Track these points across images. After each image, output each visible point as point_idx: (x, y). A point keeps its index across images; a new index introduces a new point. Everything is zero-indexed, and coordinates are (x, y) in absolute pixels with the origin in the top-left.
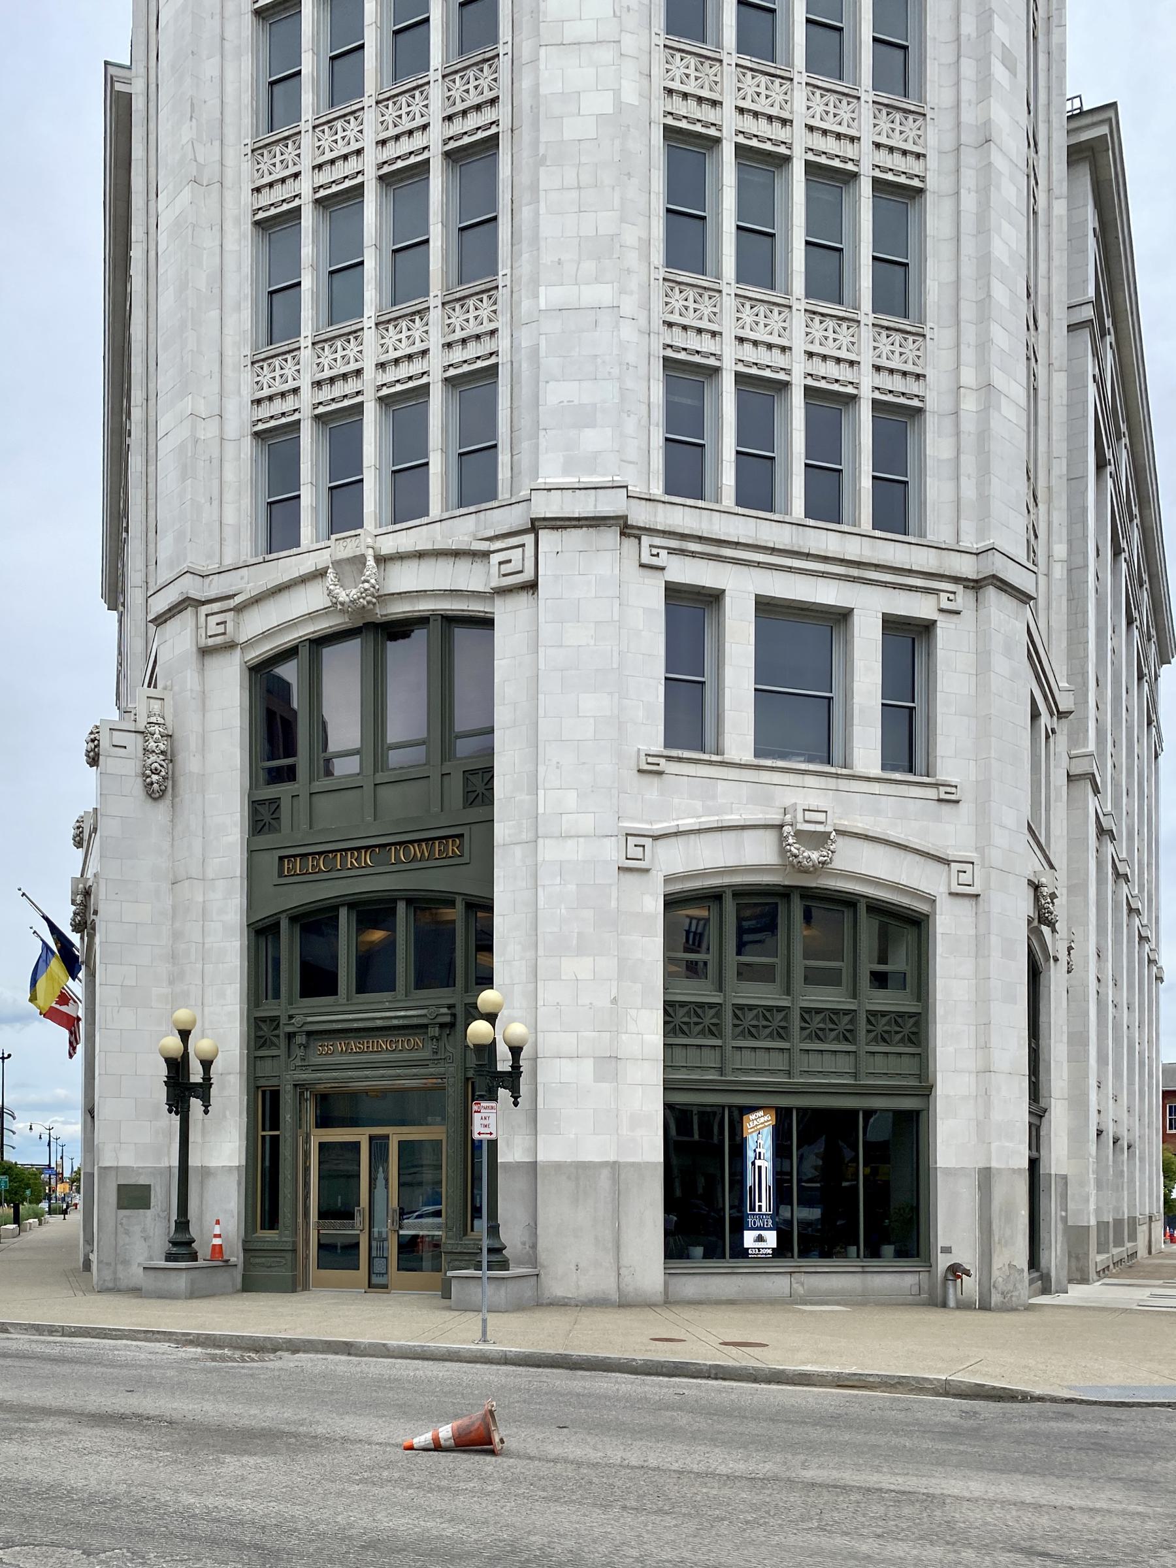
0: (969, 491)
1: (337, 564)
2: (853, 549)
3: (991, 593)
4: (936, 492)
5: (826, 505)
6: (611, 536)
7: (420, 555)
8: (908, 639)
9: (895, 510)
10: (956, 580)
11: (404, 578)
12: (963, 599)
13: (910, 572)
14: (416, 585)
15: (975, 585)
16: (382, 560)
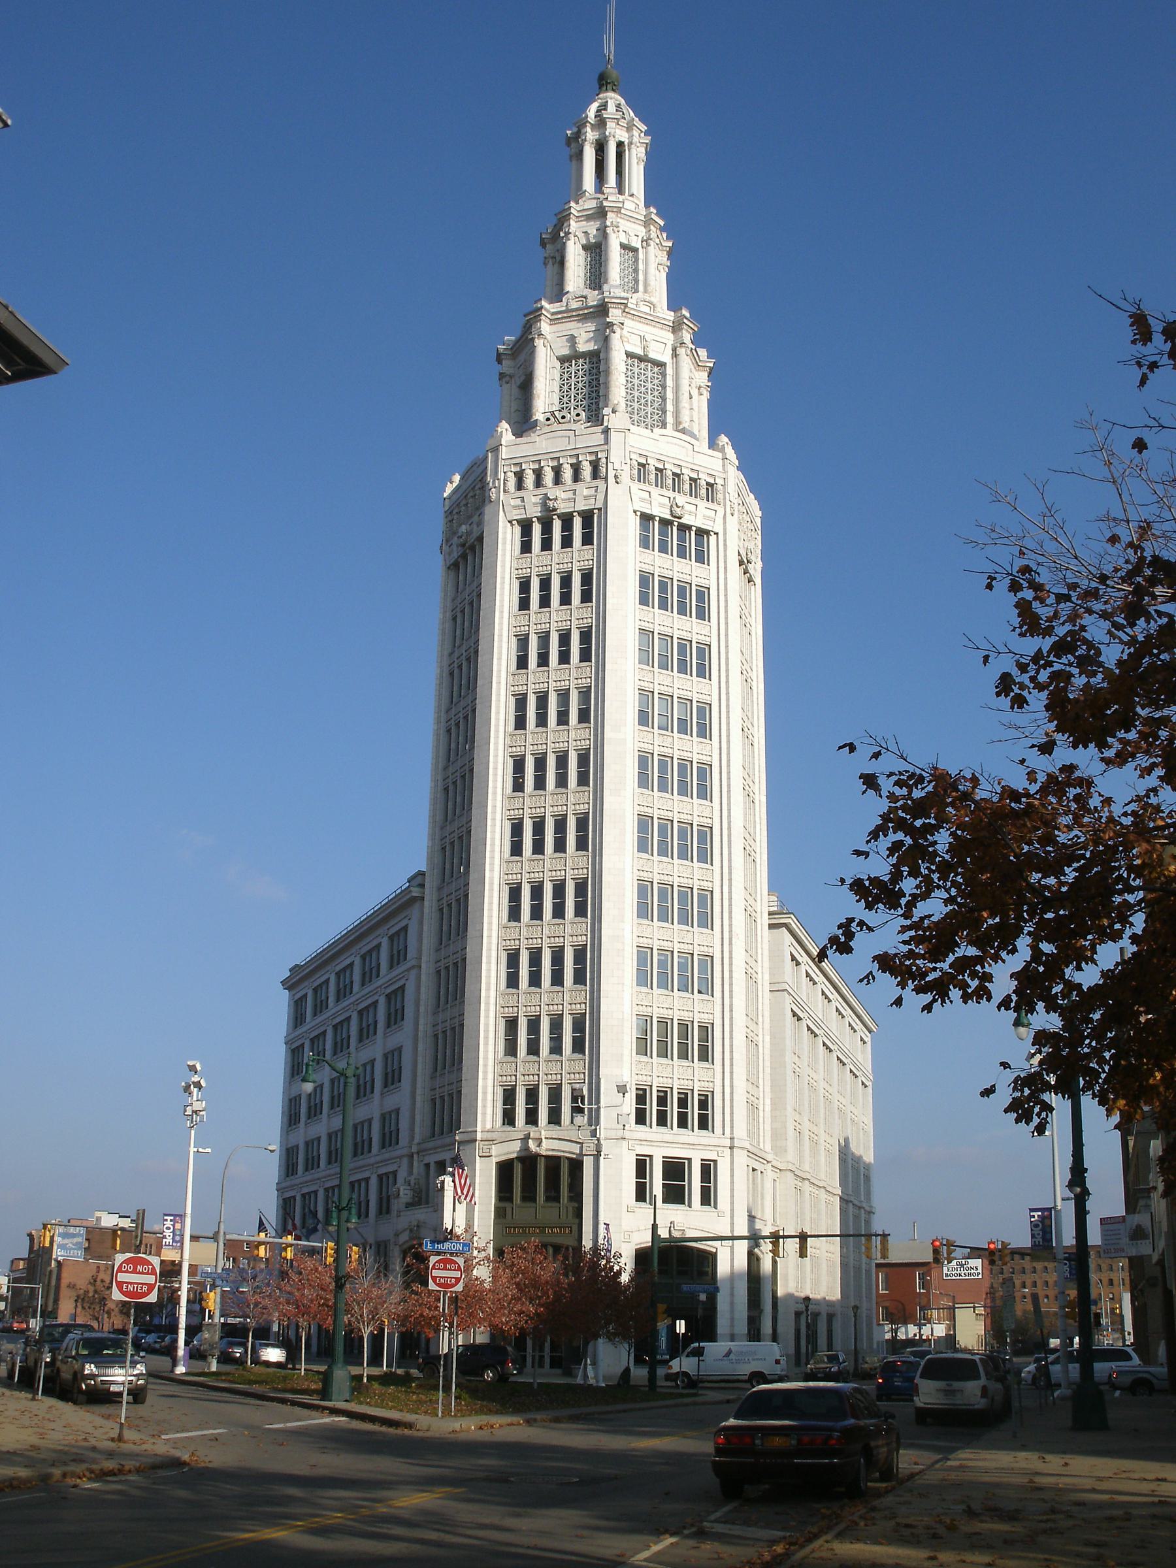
9: (704, 1124)
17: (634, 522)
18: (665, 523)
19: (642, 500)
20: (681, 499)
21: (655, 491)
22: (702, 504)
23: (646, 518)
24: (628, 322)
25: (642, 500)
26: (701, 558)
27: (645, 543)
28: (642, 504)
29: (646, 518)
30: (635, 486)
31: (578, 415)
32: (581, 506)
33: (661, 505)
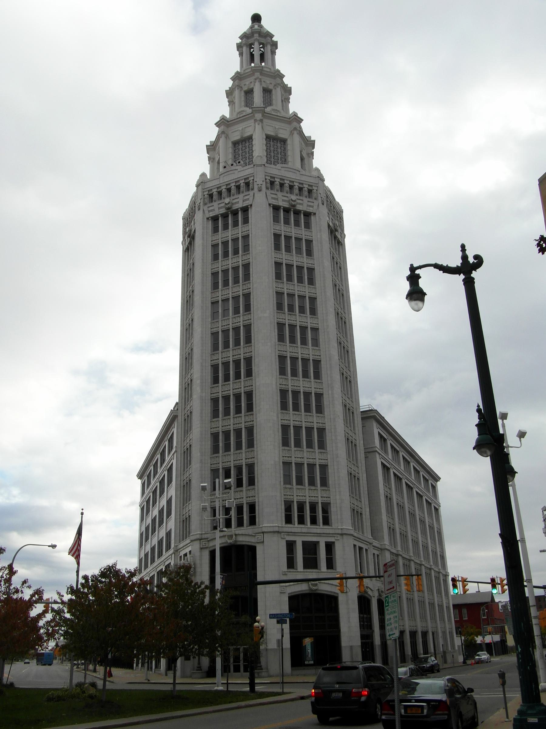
0: (339, 517)
1: (228, 536)
2: (319, 531)
3: (344, 536)
4: (334, 517)
5: (314, 521)
6: (276, 534)
7: (242, 535)
8: (330, 547)
9: (326, 521)
10: (338, 534)
11: (240, 539)
12: (339, 537)
13: (329, 534)
14: (243, 540)
15: (342, 535)
16: (236, 535)
17: (269, 212)
18: (287, 211)
19: (273, 198)
20: (294, 197)
21: (280, 194)
22: (306, 200)
23: (276, 208)
24: (265, 121)
25: (273, 198)
26: (308, 226)
27: (276, 220)
28: (273, 201)
29: (276, 208)
30: (269, 192)
31: (239, 162)
32: (240, 205)
33: (283, 200)
